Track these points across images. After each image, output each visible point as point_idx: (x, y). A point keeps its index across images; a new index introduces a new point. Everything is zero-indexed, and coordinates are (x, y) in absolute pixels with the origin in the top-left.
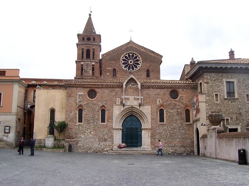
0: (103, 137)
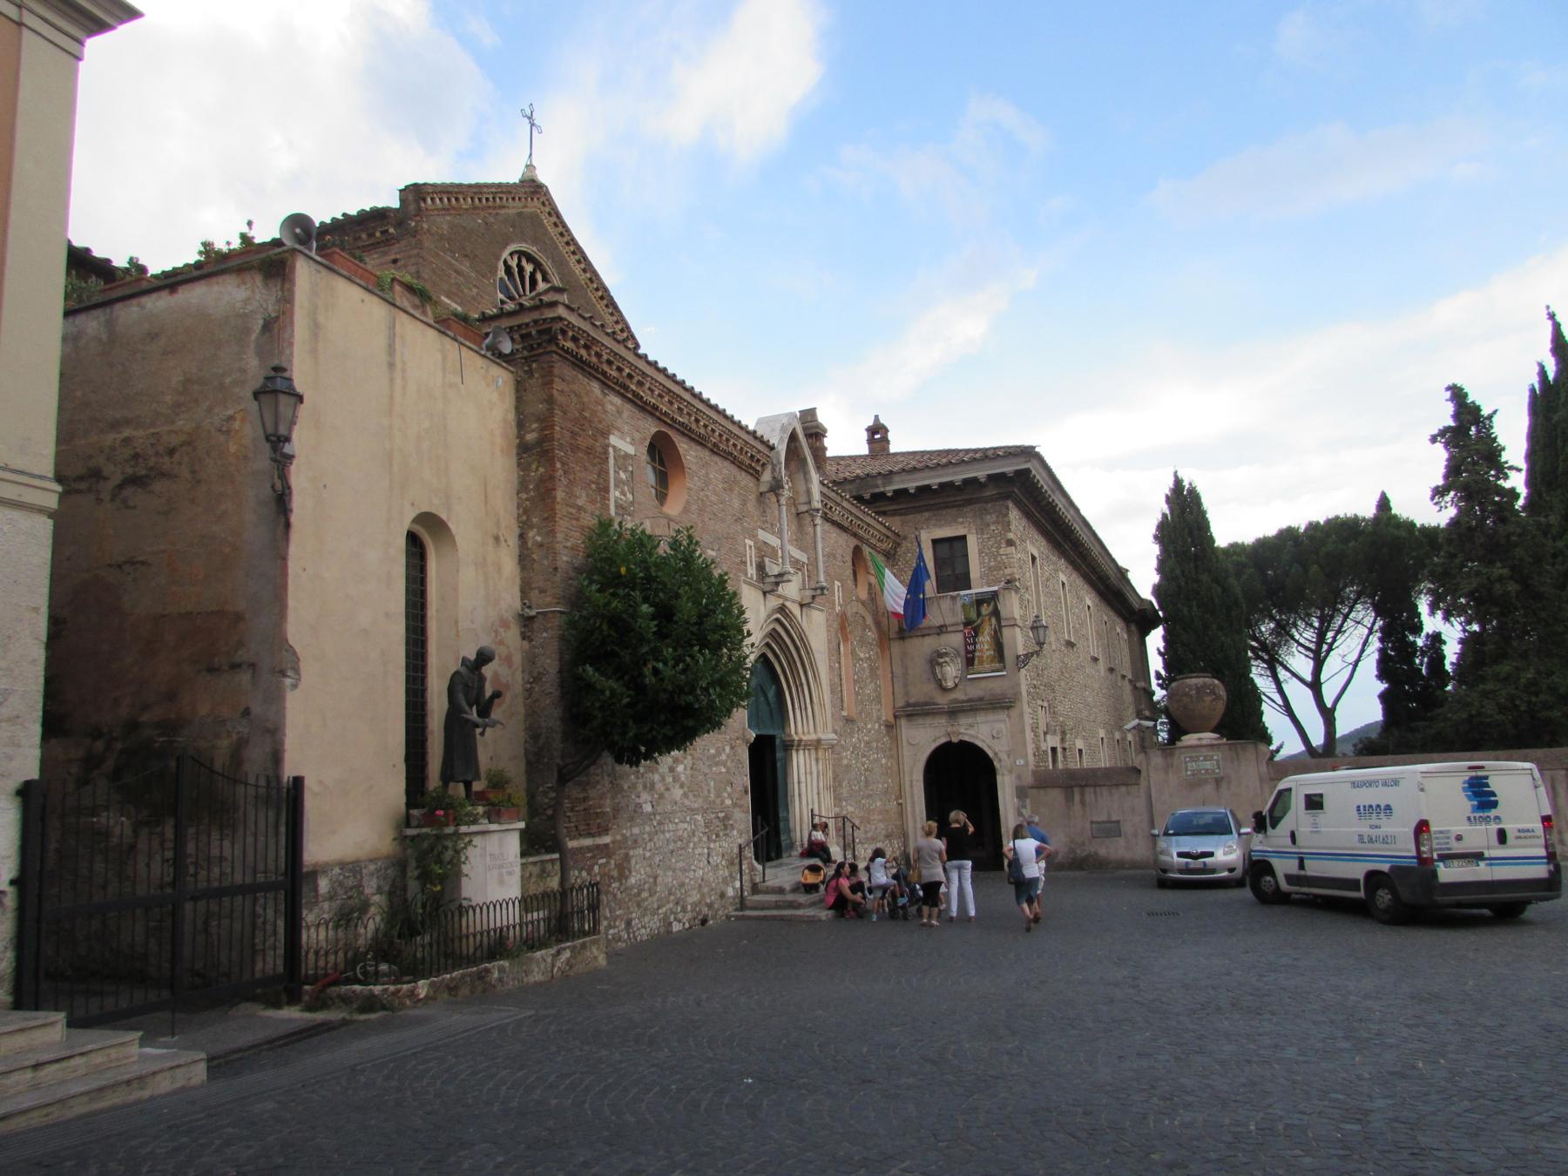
0: (718, 801)
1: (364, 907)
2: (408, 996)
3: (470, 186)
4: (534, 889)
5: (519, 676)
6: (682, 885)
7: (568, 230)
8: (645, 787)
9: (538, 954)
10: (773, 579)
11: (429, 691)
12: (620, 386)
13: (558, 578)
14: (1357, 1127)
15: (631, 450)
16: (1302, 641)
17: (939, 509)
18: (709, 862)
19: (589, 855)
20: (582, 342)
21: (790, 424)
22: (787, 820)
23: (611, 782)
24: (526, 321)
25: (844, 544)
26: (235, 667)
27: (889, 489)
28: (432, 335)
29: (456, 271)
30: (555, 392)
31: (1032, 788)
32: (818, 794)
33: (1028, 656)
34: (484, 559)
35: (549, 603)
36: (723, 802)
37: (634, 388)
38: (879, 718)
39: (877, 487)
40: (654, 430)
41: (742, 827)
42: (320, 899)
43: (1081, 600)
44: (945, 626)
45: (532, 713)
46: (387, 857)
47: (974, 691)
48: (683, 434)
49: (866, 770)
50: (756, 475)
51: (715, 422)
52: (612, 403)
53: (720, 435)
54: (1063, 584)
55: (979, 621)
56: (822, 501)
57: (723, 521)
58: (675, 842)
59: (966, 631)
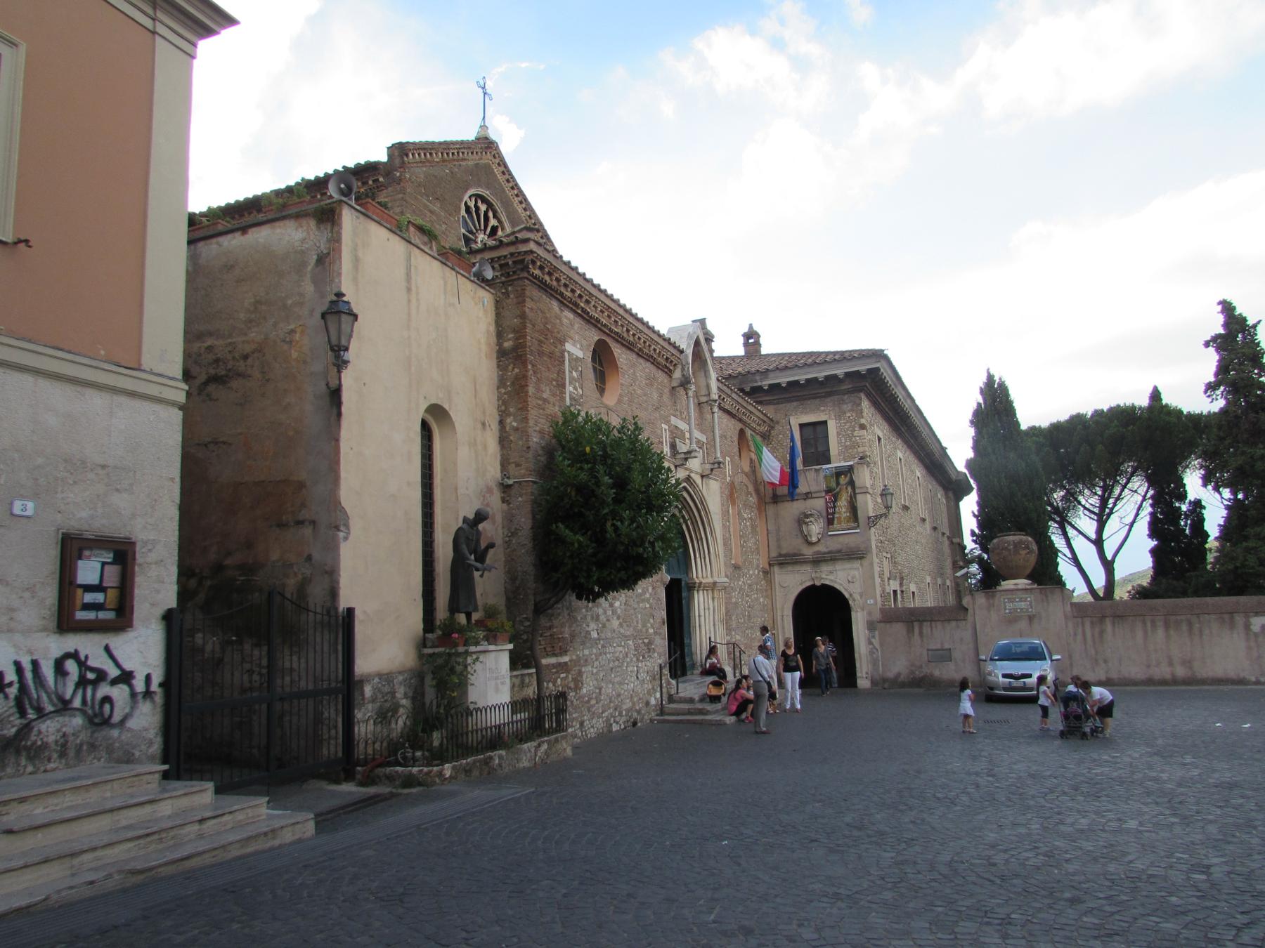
0: (644, 630)
1: (395, 708)
2: (437, 776)
3: (440, 143)
4: (518, 697)
5: (500, 531)
6: (619, 695)
7: (513, 177)
8: (592, 618)
9: (525, 746)
10: (683, 456)
11: (436, 542)
12: (573, 304)
13: (530, 455)
14: (1203, 877)
15: (580, 354)
16: (1087, 506)
17: (806, 399)
18: (637, 678)
19: (554, 670)
20: (547, 270)
21: (695, 333)
22: (690, 646)
23: (569, 614)
24: (505, 253)
25: (732, 427)
26: (300, 523)
27: (765, 384)
28: (436, 264)
29: (431, 212)
30: (527, 310)
31: (880, 622)
32: (714, 625)
33: (878, 517)
34: (475, 440)
35: (524, 474)
36: (647, 631)
37: (582, 305)
38: (758, 566)
39: (756, 382)
40: (596, 338)
41: (661, 650)
42: (366, 702)
43: (913, 472)
44: (810, 493)
45: (510, 560)
46: (410, 670)
47: (833, 545)
48: (617, 341)
49: (749, 607)
50: (669, 373)
51: (641, 331)
52: (566, 316)
53: (645, 342)
54: (900, 459)
55: (838, 489)
56: (720, 396)
57: (646, 409)
58: (614, 662)
59: (828, 497)
